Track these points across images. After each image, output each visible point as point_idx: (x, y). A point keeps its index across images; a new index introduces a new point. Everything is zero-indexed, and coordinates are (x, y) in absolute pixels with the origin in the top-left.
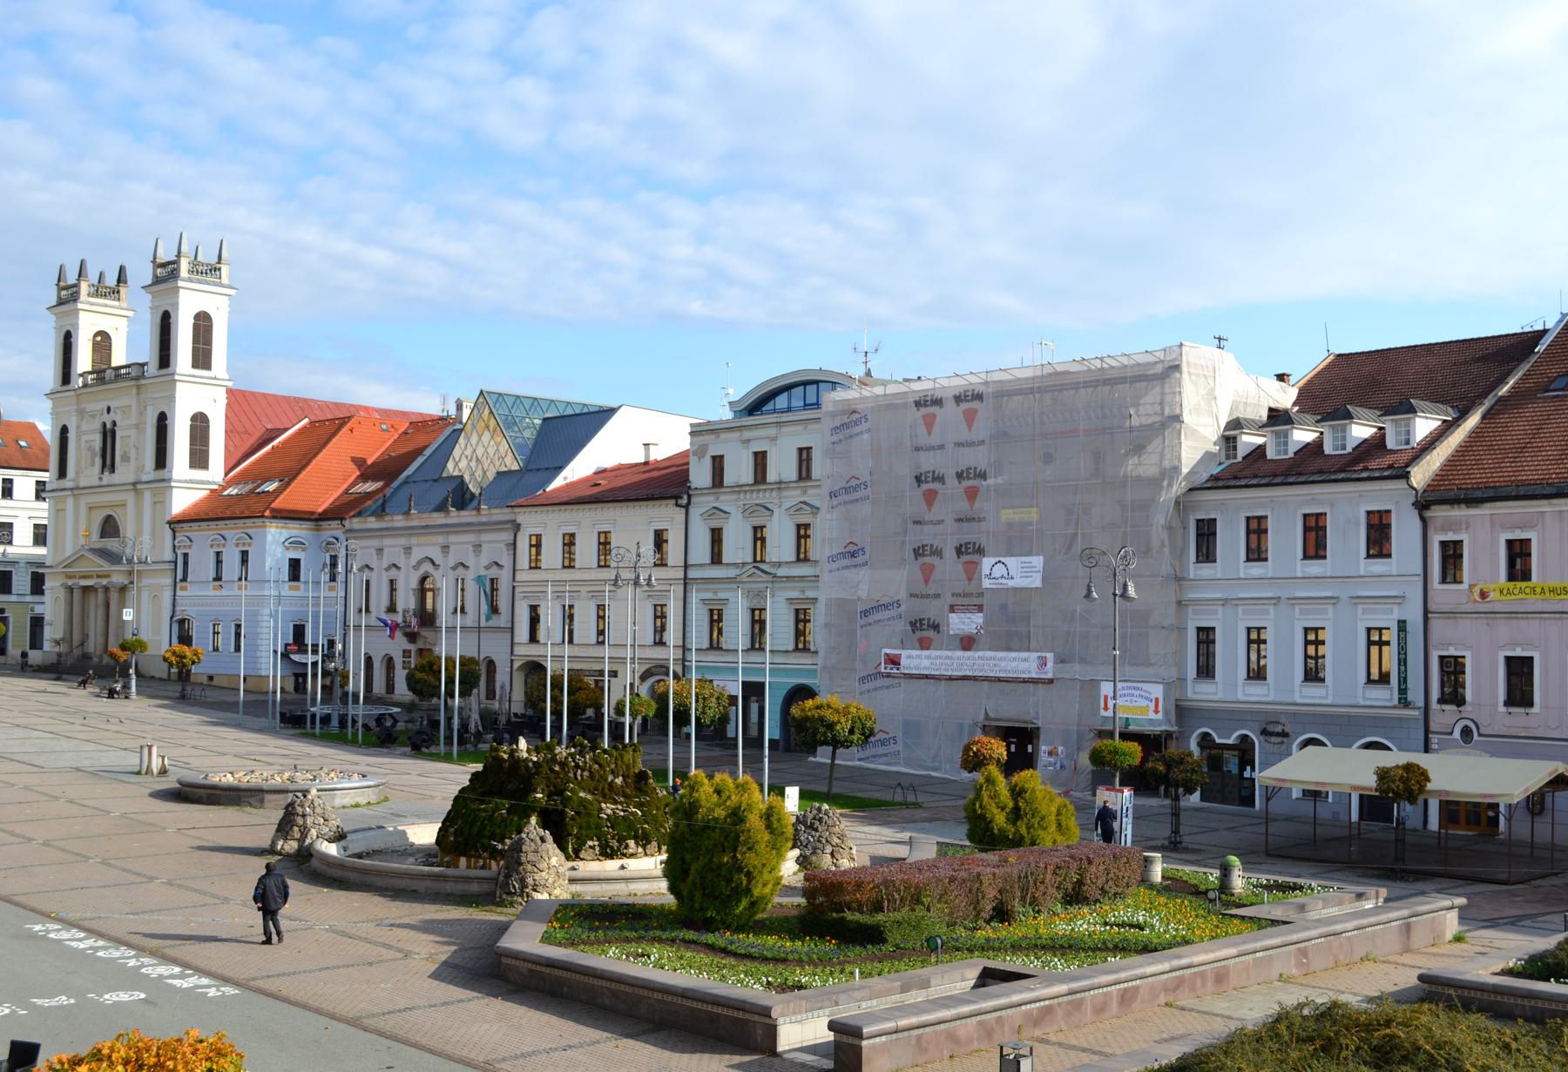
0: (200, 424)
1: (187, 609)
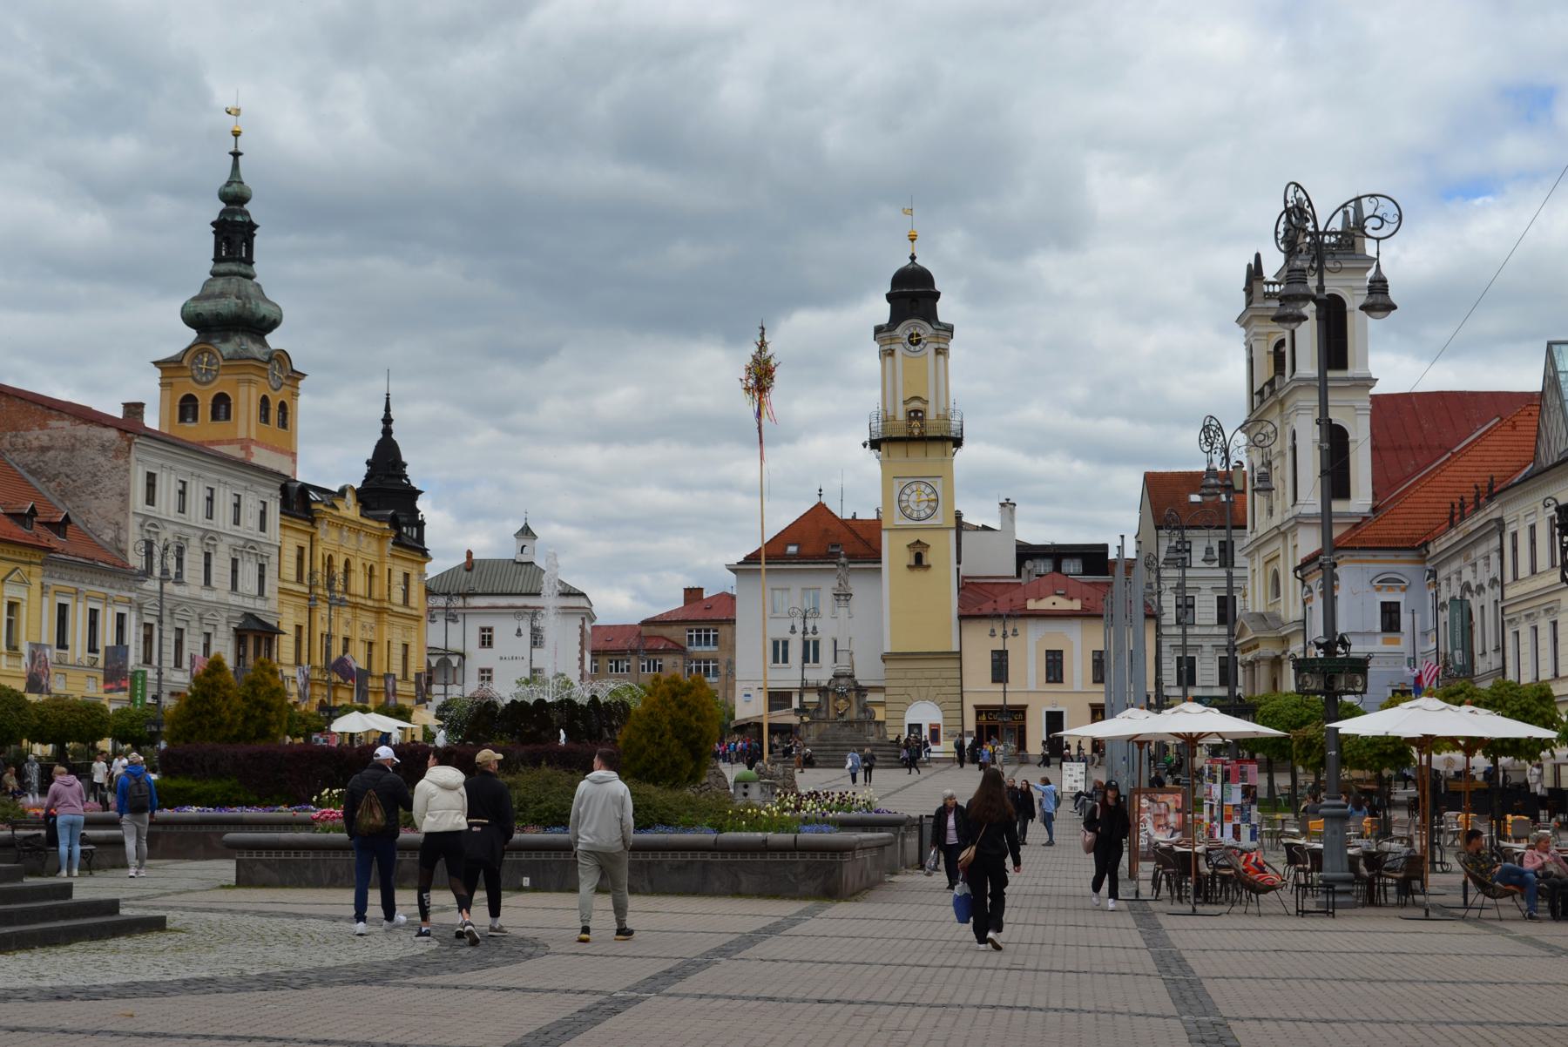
0: (1336, 442)
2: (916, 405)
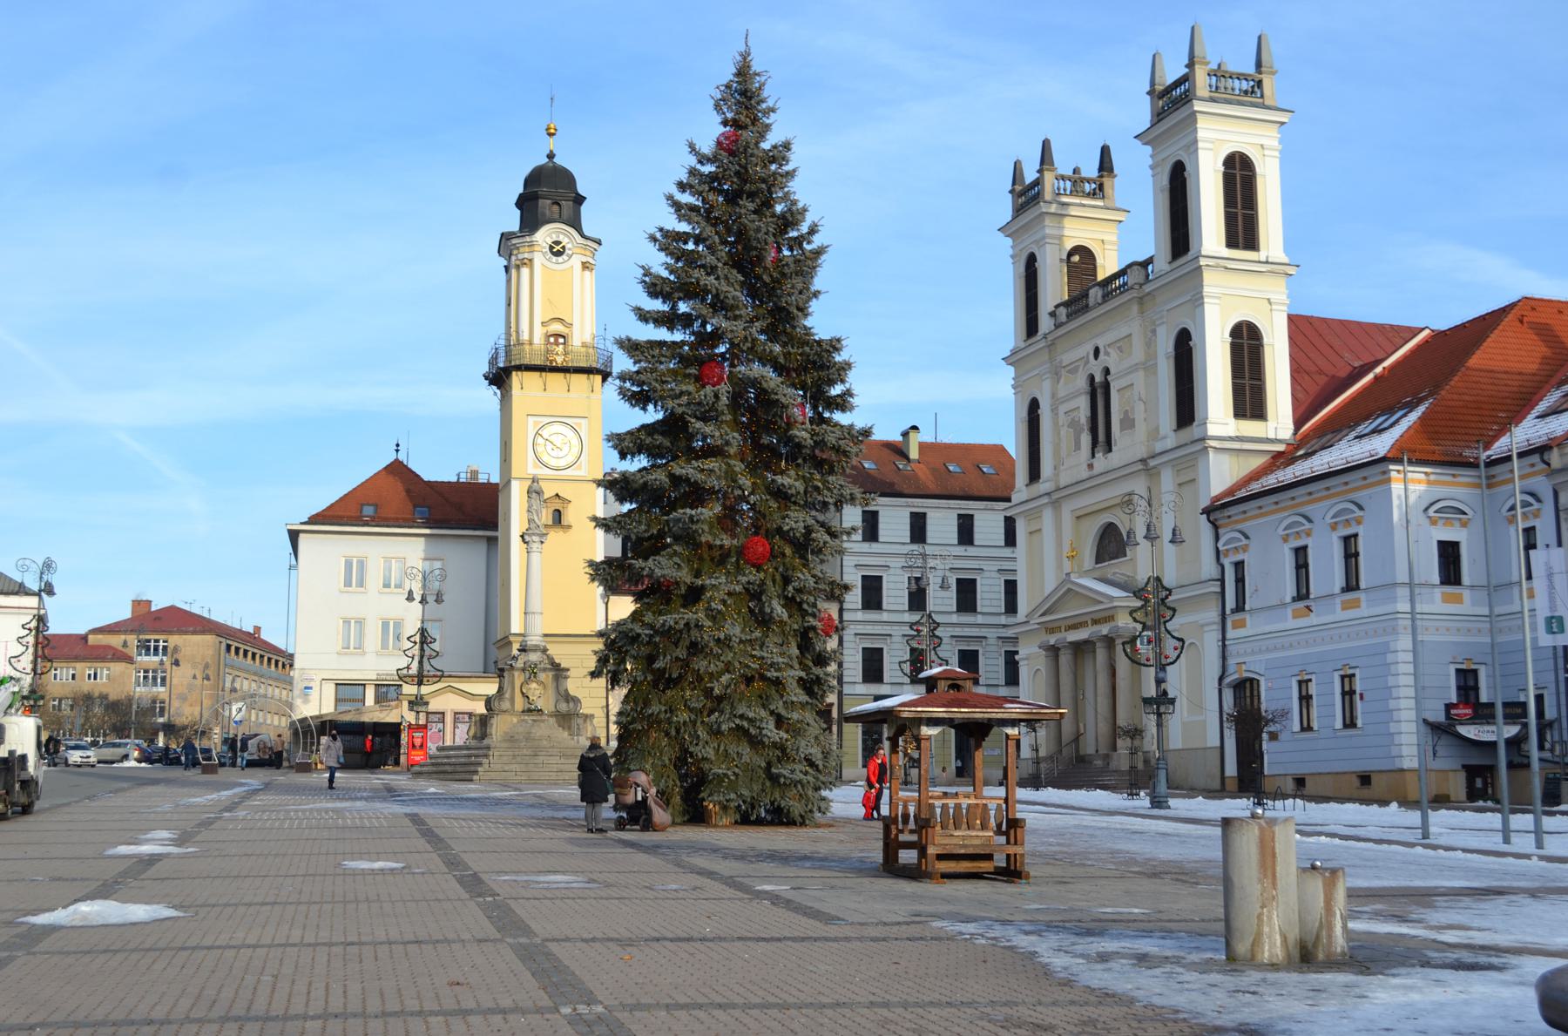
0: (1246, 341)
1: (1247, 662)
2: (557, 327)
